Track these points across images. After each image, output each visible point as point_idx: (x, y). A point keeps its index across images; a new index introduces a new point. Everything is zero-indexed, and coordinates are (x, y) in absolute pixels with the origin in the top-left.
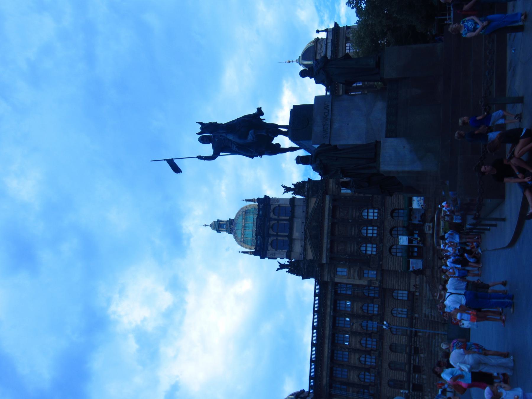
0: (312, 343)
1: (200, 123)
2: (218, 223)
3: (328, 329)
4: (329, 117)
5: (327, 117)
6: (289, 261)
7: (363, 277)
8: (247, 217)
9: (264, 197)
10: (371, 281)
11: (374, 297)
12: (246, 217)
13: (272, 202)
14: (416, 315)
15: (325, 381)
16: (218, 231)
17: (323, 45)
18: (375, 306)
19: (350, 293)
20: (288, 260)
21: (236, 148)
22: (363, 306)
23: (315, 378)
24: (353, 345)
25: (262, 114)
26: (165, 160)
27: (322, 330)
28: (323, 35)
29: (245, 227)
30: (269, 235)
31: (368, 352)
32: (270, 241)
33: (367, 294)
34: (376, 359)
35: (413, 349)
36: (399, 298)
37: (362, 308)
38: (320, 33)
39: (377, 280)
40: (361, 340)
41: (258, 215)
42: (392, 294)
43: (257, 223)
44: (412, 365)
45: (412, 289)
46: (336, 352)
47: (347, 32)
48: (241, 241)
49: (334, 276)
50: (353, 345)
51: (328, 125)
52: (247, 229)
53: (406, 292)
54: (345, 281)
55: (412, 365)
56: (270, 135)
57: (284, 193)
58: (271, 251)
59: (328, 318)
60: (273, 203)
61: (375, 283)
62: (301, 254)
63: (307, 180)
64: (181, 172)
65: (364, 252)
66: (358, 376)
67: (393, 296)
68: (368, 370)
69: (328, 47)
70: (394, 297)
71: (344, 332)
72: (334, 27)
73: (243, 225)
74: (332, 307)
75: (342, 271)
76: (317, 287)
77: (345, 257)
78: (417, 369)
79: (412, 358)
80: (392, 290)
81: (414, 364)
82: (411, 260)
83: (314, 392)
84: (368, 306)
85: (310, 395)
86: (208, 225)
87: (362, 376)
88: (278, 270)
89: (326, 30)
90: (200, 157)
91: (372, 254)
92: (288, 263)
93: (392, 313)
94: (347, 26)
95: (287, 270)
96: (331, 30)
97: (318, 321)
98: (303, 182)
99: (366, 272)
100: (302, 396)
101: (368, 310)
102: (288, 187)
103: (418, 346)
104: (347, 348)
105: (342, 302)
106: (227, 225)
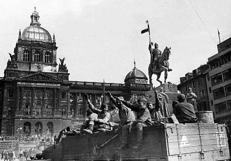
9: (57, 47)
16: (31, 16)
26: (148, 26)
57: (60, 59)
63: (69, 73)
86: (35, 9)
95: (10, 60)
98: (67, 70)
102: (64, 61)
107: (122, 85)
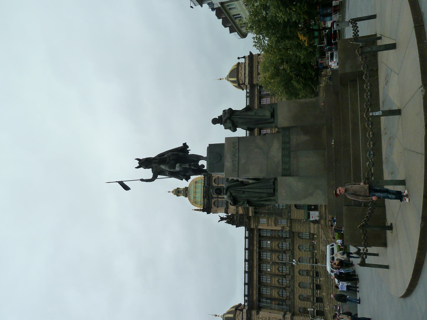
0: (245, 271)
1: (138, 159)
2: (177, 190)
3: (255, 261)
5: (236, 155)
6: (227, 215)
7: (278, 224)
8: (197, 185)
10: (283, 227)
11: (286, 238)
12: (196, 185)
13: (213, 175)
14: (316, 251)
15: (255, 297)
16: (177, 196)
17: (243, 67)
18: (287, 243)
19: (270, 235)
20: (226, 214)
21: (168, 174)
22: (279, 244)
23: (248, 296)
24: (273, 271)
25: (188, 147)
26: (116, 182)
27: (252, 262)
28: (242, 61)
29: (195, 192)
30: (212, 198)
32: (213, 201)
33: (281, 236)
34: (289, 280)
35: (315, 273)
36: (303, 238)
37: (278, 245)
38: (240, 59)
39: (287, 226)
40: (279, 267)
41: (204, 184)
42: (298, 235)
43: (203, 189)
44: (315, 284)
45: (312, 232)
46: (261, 276)
47: (258, 57)
48: (193, 202)
49: (258, 225)
50: (273, 271)
51: (236, 161)
52: (197, 193)
53: (308, 233)
54: (265, 228)
55: (315, 284)
56: (192, 168)
58: (214, 208)
59: (255, 253)
60: (214, 176)
61: (286, 228)
62: (234, 210)
64: (130, 189)
65: (278, 207)
66: (278, 293)
67: (299, 237)
69: (246, 68)
70: (300, 237)
71: (267, 263)
72: (249, 55)
73: (194, 191)
74: (258, 245)
75: (263, 220)
76: (247, 232)
77: (265, 211)
78: (318, 287)
79: (315, 279)
80: (299, 233)
81: (317, 283)
82: (311, 212)
83: (248, 305)
84: (282, 244)
85: (245, 307)
86: (171, 192)
88: (219, 221)
89: (244, 57)
90: (142, 180)
91: (283, 209)
92: (226, 217)
93: (299, 248)
94: (258, 54)
95: (226, 221)
96: (248, 57)
97: (249, 256)
99: (279, 221)
100: (240, 308)
101: (282, 247)
103: (318, 271)
104: (269, 274)
105: (264, 242)
106: (183, 191)
107: (247, 93)
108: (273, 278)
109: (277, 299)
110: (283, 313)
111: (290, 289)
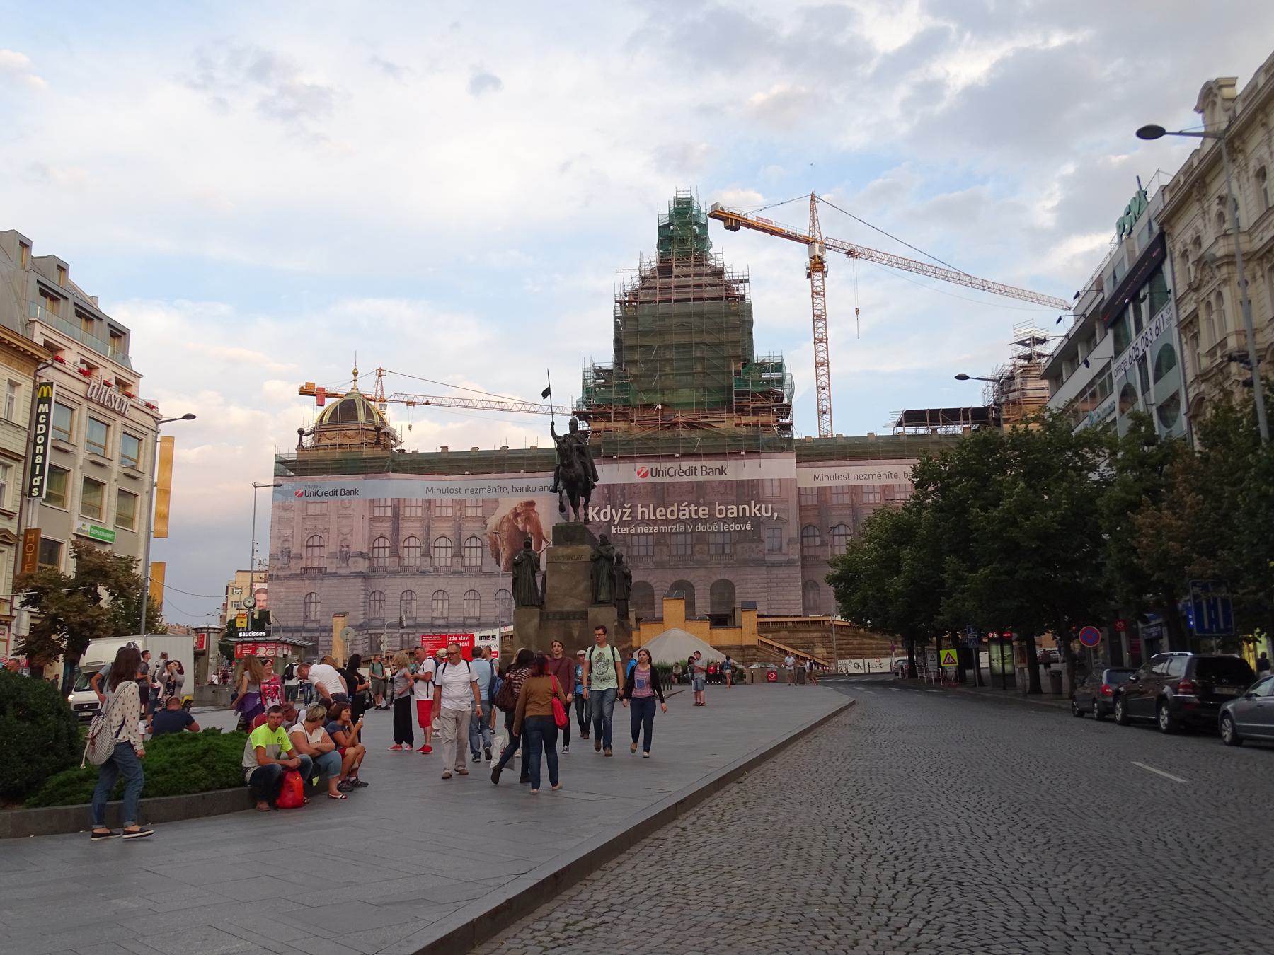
4: (571, 560)
31: (458, 554)
68: (426, 554)
87: (412, 542)
108: (450, 524)
109: (398, 534)
110: (365, 551)
111: (428, 568)
